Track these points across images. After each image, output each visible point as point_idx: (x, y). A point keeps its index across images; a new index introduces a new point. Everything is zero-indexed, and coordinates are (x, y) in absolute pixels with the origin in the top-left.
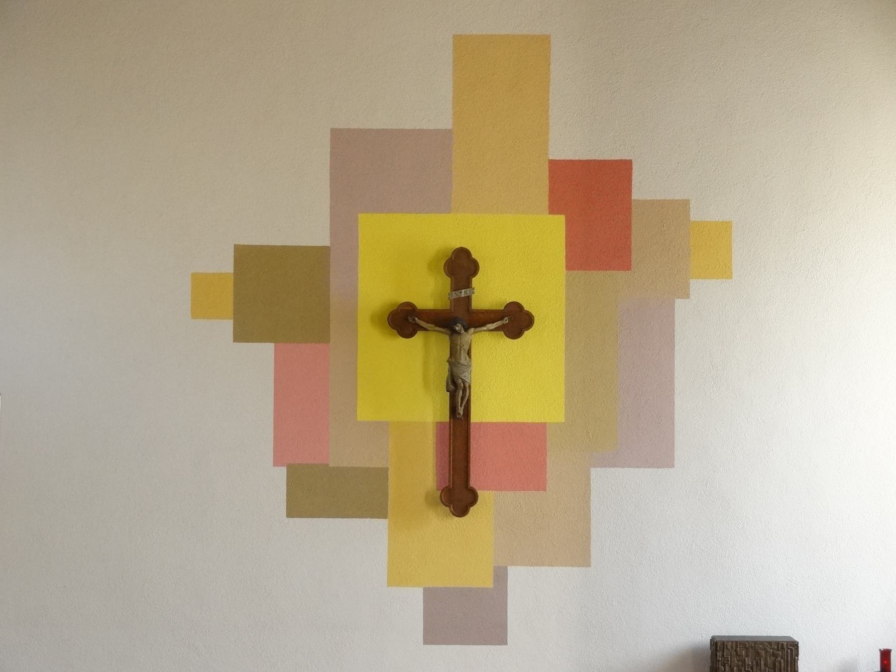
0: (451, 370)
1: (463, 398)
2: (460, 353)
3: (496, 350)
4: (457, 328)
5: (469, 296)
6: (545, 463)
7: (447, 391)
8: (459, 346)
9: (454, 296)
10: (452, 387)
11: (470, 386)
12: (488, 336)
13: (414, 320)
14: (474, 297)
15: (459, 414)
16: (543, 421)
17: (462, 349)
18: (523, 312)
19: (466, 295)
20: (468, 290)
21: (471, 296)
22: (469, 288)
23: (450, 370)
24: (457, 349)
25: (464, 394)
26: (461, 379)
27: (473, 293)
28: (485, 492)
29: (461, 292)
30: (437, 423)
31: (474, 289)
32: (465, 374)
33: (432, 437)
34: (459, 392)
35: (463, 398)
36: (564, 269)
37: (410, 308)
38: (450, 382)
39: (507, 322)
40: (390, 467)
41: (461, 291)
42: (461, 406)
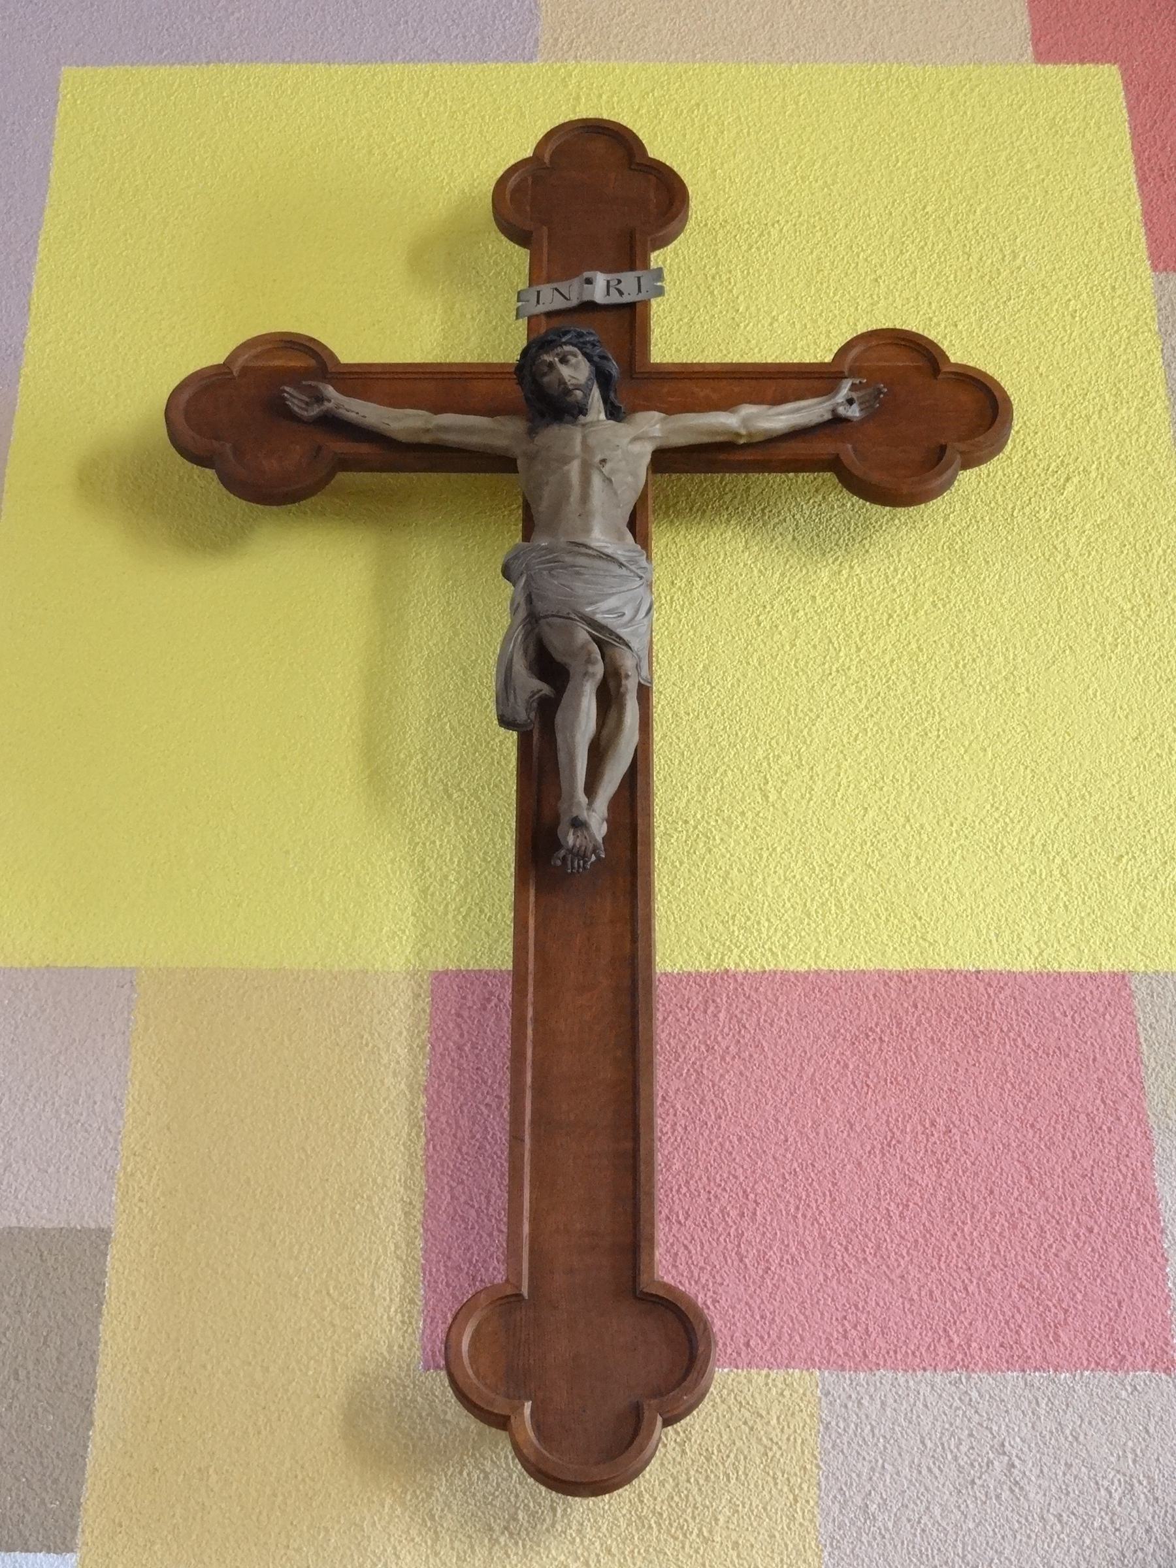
0: (529, 599)
1: (599, 752)
2: (585, 498)
3: (794, 612)
4: (565, 371)
5: (632, 306)
6: (1149, 1200)
7: (505, 722)
8: (574, 468)
9: (550, 299)
10: (530, 685)
11: (644, 693)
12: (746, 548)
13: (320, 399)
14: (657, 307)
15: (578, 824)
16: (1109, 964)
17: (597, 481)
18: (945, 369)
19: (615, 298)
20: (628, 279)
21: (646, 304)
22: (632, 268)
23: (521, 599)
24: (565, 482)
25: (613, 714)
26: (592, 623)
27: (660, 292)
28: (758, 1376)
29: (589, 281)
30: (439, 977)
31: (659, 274)
32: (612, 602)
33: (403, 1052)
34: (576, 708)
35: (599, 752)
36: (1144, 267)
37: (298, 362)
38: (520, 667)
39: (854, 412)
40: (118, 1230)
41: (587, 274)
42: (591, 789)
